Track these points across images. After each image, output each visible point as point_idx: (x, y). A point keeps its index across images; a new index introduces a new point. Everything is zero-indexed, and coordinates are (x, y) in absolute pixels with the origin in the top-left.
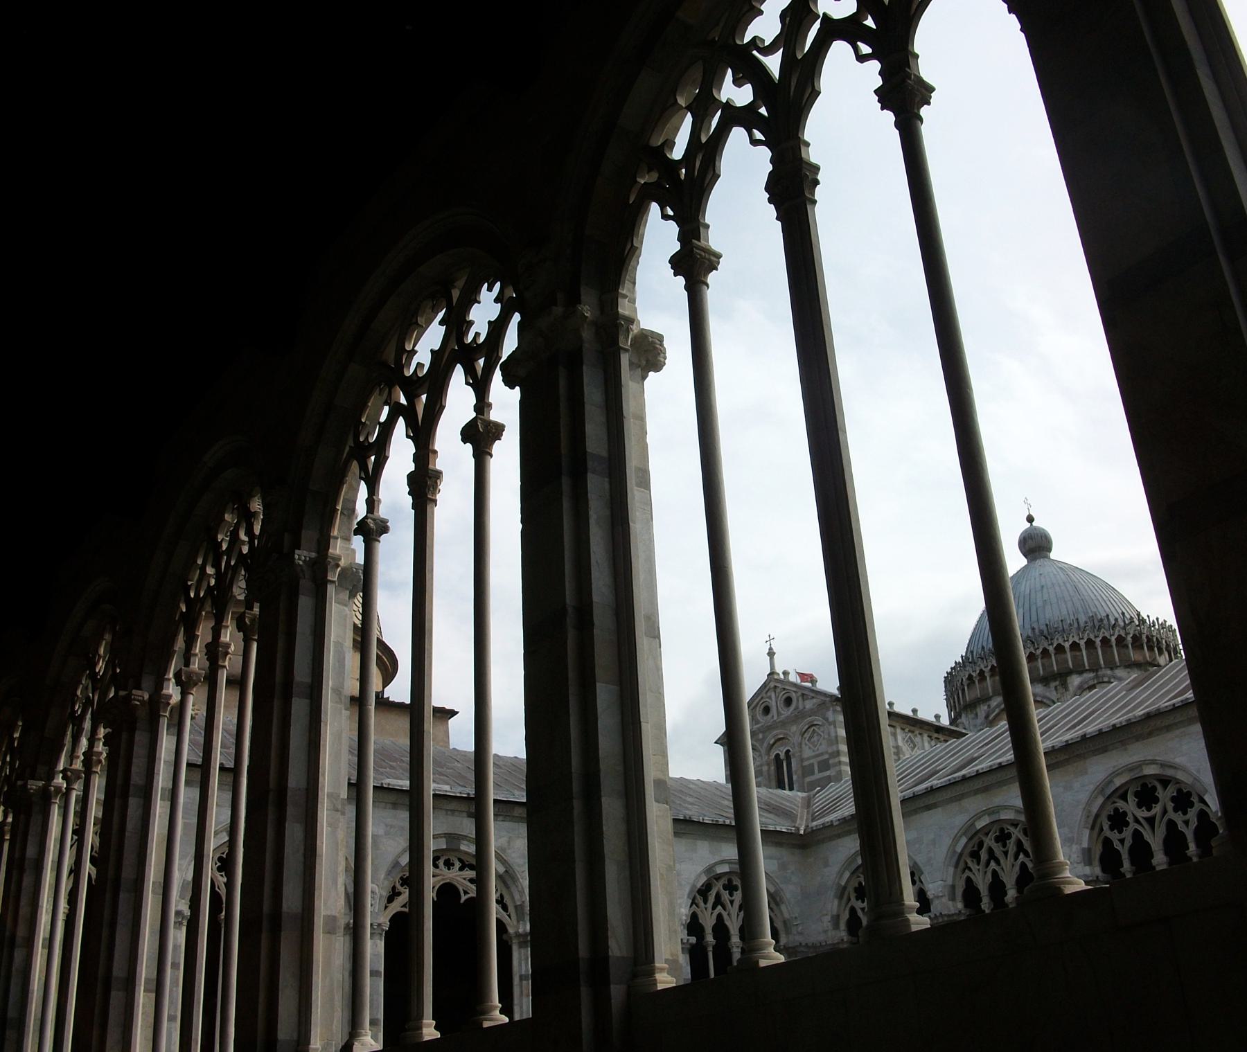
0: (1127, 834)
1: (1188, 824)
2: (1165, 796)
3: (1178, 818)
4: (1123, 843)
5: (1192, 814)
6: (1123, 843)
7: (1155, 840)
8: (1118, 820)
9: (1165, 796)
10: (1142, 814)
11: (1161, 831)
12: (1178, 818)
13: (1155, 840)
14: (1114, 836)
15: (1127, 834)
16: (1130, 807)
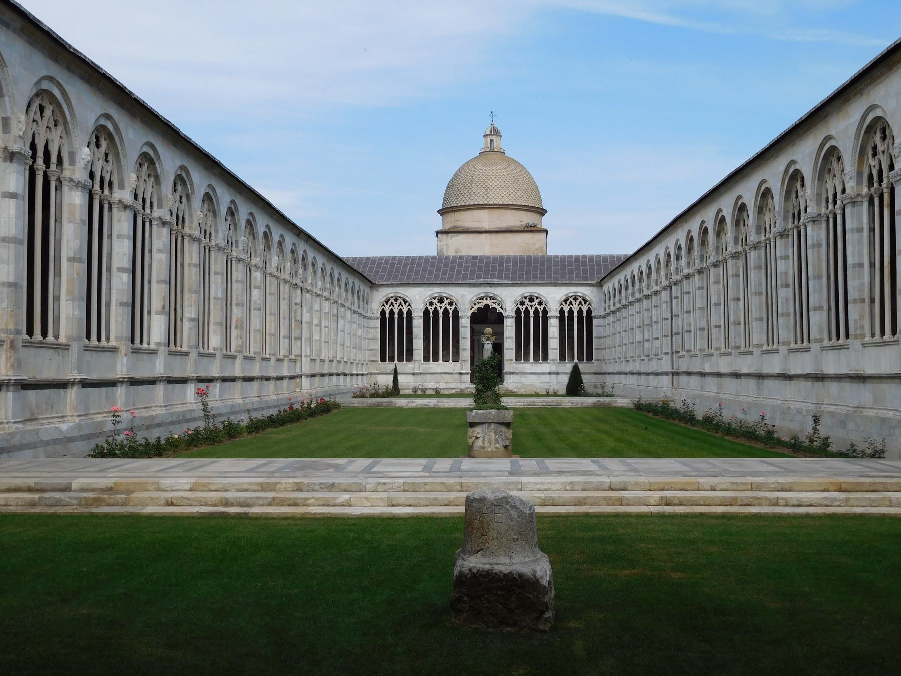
0: (524, 307)
1: (540, 309)
2: (536, 301)
3: (538, 307)
4: (522, 309)
5: (542, 307)
6: (522, 309)
7: (531, 311)
8: (522, 304)
9: (536, 301)
10: (529, 304)
11: (533, 309)
12: (538, 307)
13: (531, 311)
14: (520, 307)
15: (524, 307)
16: (527, 301)
